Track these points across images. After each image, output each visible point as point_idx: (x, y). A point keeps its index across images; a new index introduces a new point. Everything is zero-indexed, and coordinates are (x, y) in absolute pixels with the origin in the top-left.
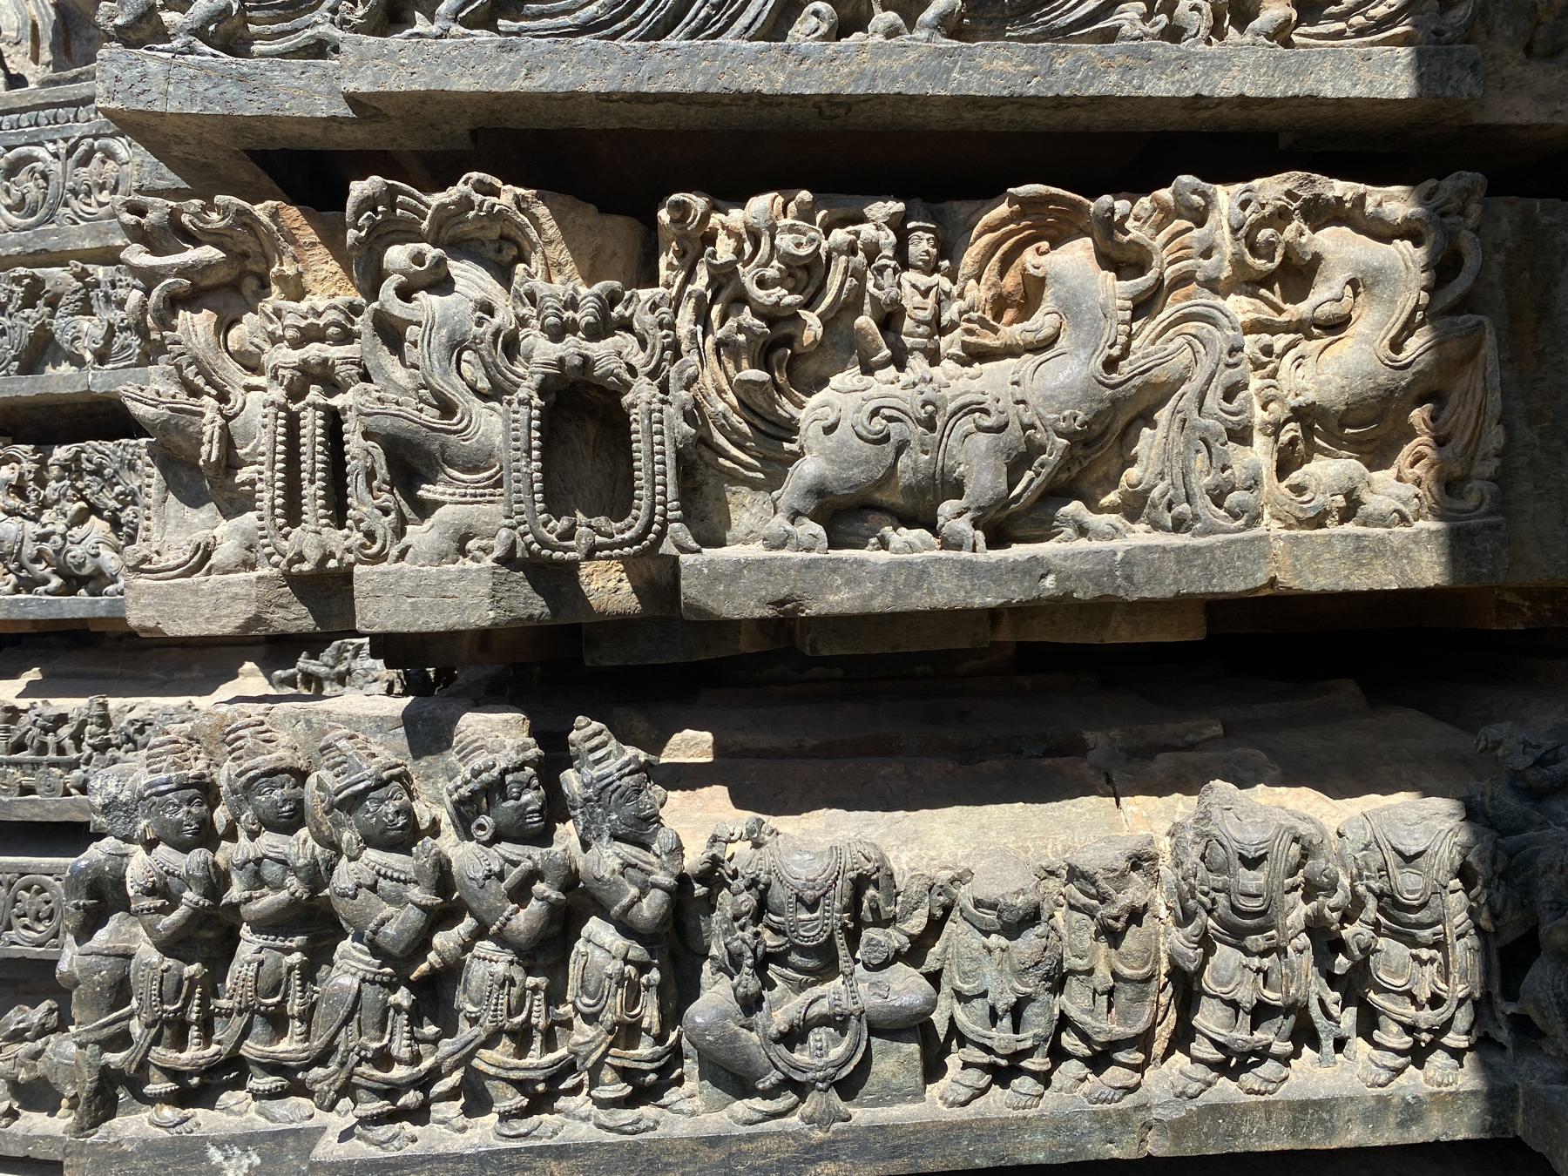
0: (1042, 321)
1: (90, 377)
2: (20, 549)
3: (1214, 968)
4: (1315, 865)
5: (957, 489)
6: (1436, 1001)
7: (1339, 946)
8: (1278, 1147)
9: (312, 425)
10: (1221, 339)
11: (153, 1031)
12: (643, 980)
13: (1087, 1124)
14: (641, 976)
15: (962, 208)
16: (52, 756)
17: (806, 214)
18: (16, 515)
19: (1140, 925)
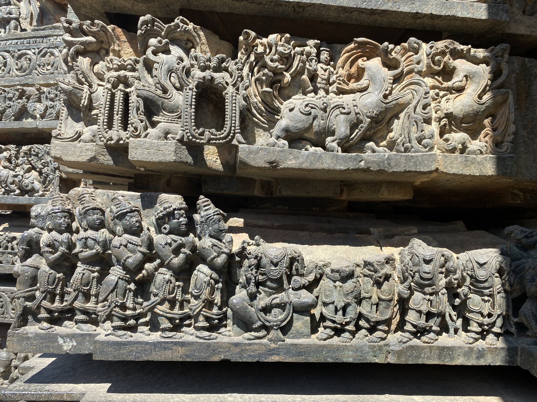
0: (363, 82)
1: (38, 123)
2: (7, 180)
3: (413, 300)
4: (449, 264)
5: (333, 133)
6: (490, 315)
7: (457, 295)
8: (434, 363)
9: (119, 96)
10: (422, 90)
11: (44, 294)
12: (216, 286)
13: (367, 349)
14: (215, 285)
15: (339, 46)
16: (9, 250)
17: (288, 42)
18: (7, 168)
19: (388, 281)
